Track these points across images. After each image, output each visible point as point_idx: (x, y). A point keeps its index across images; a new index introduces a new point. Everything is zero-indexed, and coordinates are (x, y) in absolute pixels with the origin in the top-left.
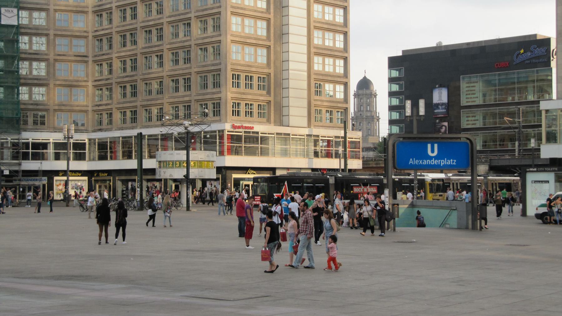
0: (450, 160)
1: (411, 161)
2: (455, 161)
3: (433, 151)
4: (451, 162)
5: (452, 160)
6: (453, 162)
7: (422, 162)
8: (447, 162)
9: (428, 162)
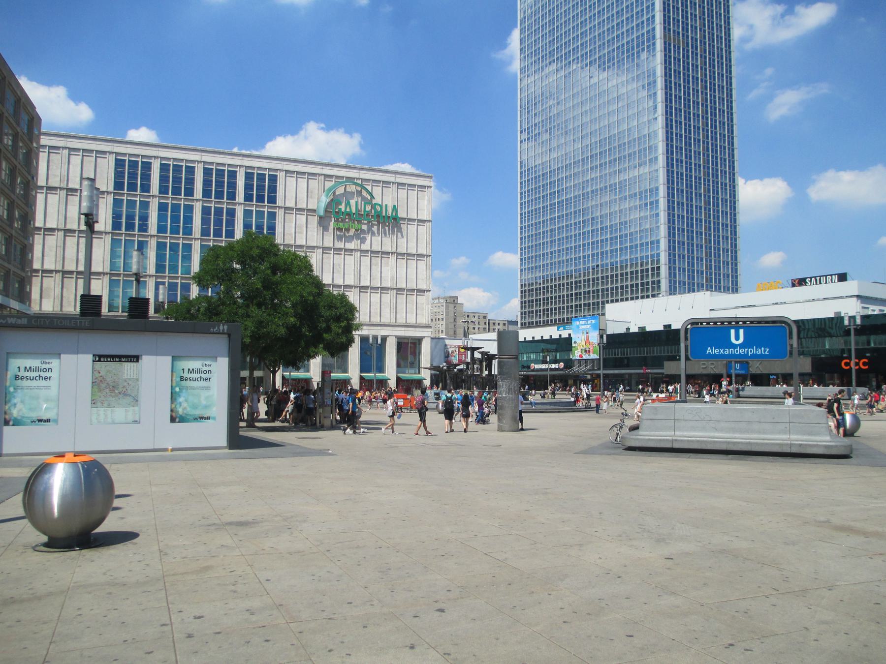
0: (761, 348)
3: (737, 338)
5: (763, 349)
7: (724, 351)
8: (756, 351)
9: (732, 351)
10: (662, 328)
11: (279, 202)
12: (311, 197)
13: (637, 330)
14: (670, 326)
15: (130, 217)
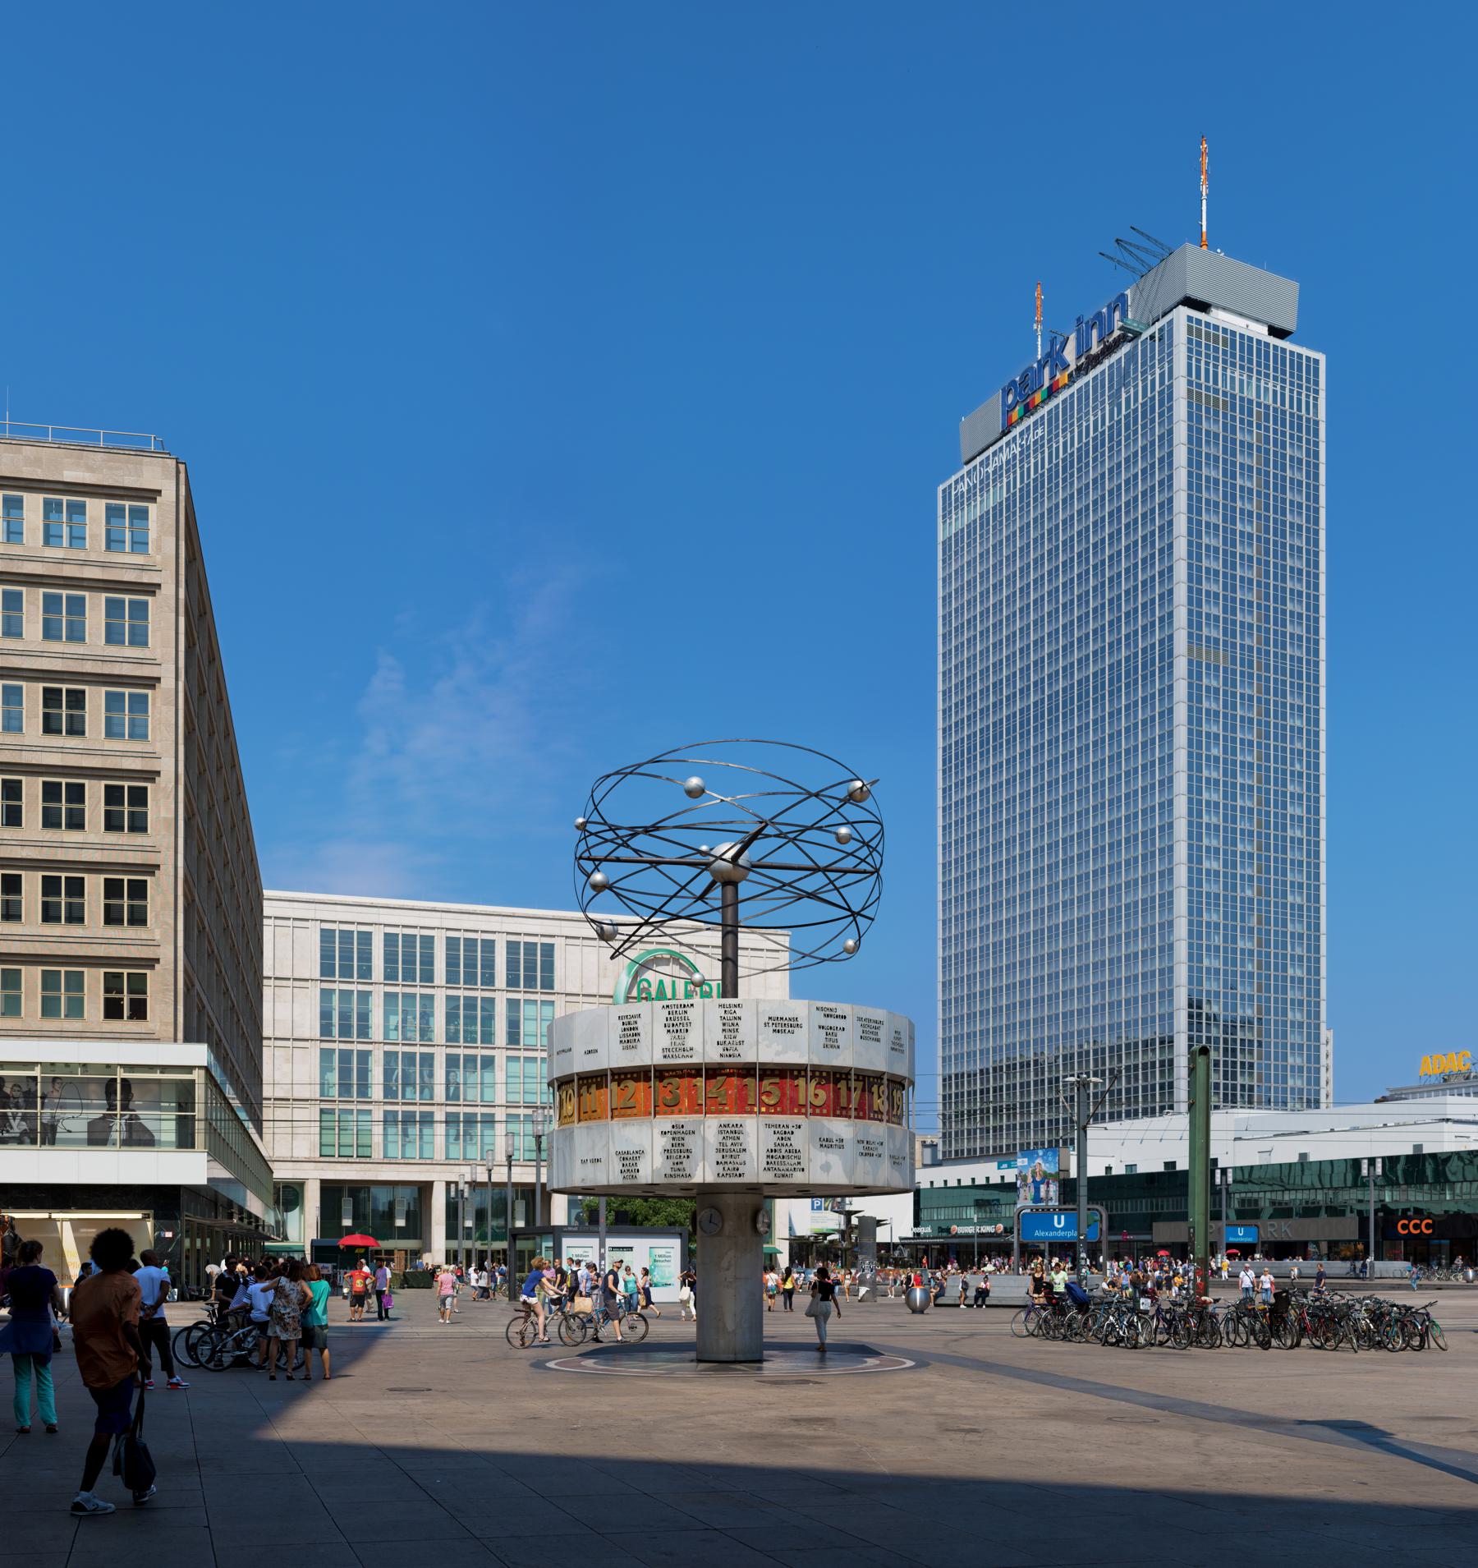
10: (1161, 1169)
11: (557, 988)
12: (605, 977)
13: (1122, 1171)
14: (1173, 1164)
15: (345, 1016)
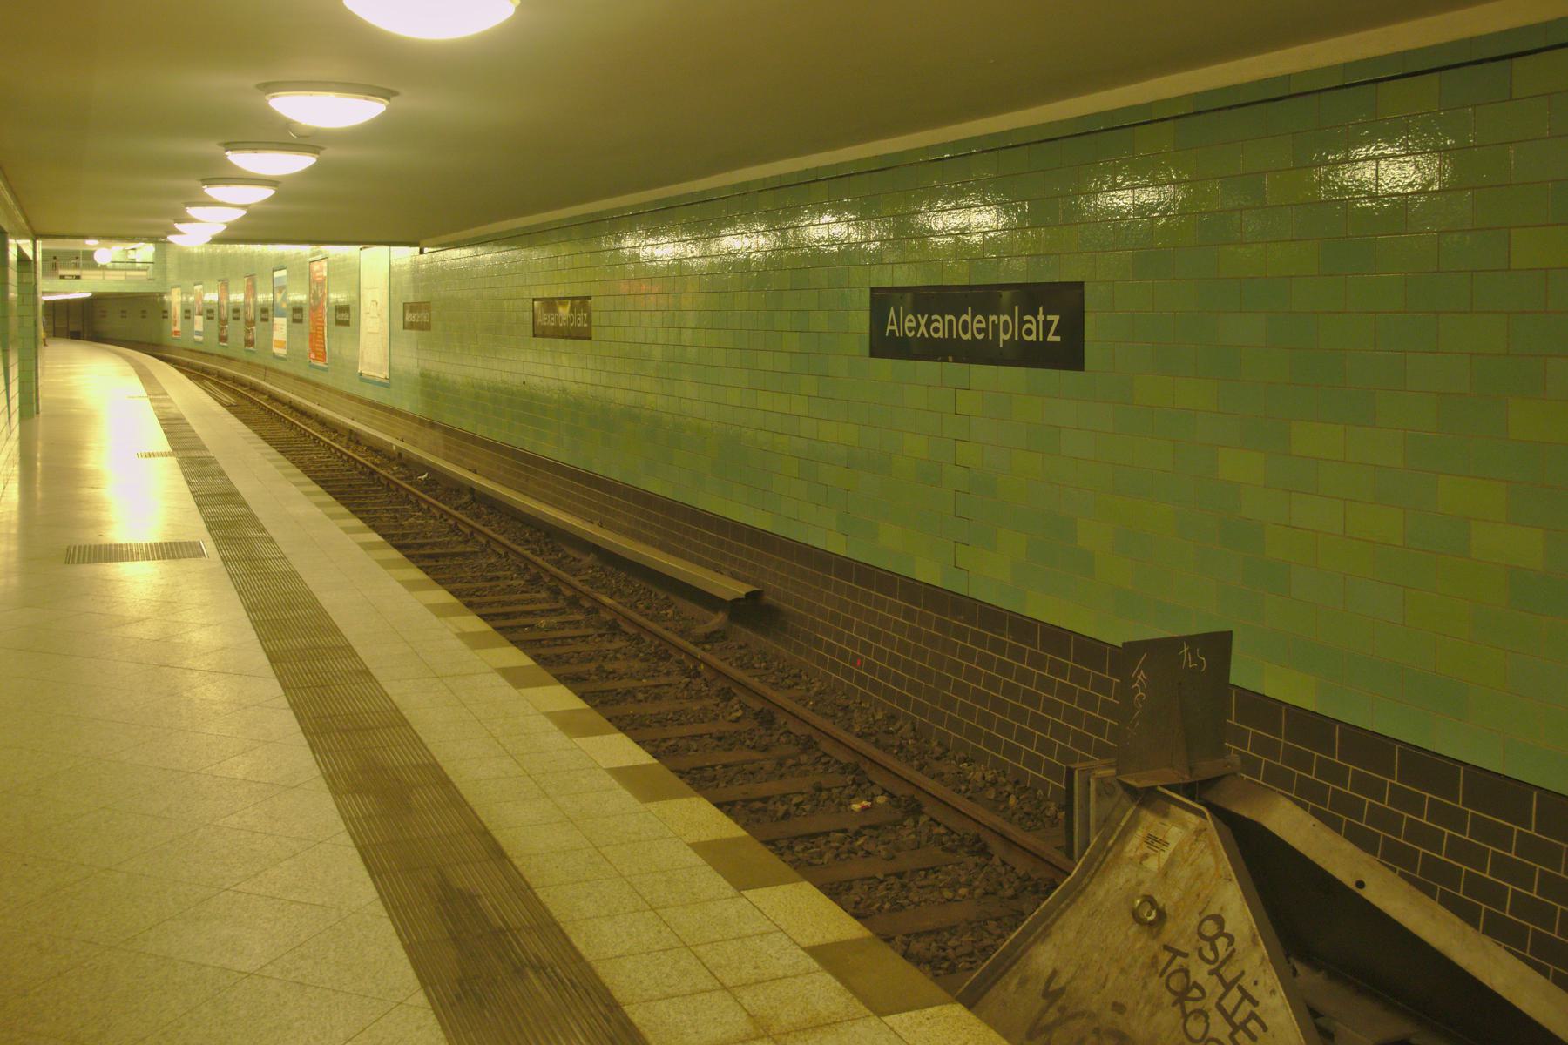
0: (1035, 315)
1: (892, 324)
2: (1055, 319)
4: (1038, 322)
6: (1047, 325)
7: (928, 326)
8: (1022, 323)
9: (950, 322)
